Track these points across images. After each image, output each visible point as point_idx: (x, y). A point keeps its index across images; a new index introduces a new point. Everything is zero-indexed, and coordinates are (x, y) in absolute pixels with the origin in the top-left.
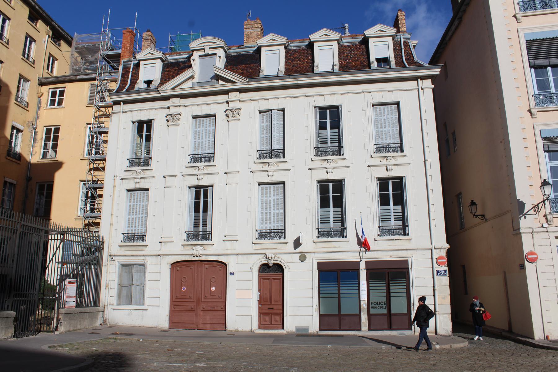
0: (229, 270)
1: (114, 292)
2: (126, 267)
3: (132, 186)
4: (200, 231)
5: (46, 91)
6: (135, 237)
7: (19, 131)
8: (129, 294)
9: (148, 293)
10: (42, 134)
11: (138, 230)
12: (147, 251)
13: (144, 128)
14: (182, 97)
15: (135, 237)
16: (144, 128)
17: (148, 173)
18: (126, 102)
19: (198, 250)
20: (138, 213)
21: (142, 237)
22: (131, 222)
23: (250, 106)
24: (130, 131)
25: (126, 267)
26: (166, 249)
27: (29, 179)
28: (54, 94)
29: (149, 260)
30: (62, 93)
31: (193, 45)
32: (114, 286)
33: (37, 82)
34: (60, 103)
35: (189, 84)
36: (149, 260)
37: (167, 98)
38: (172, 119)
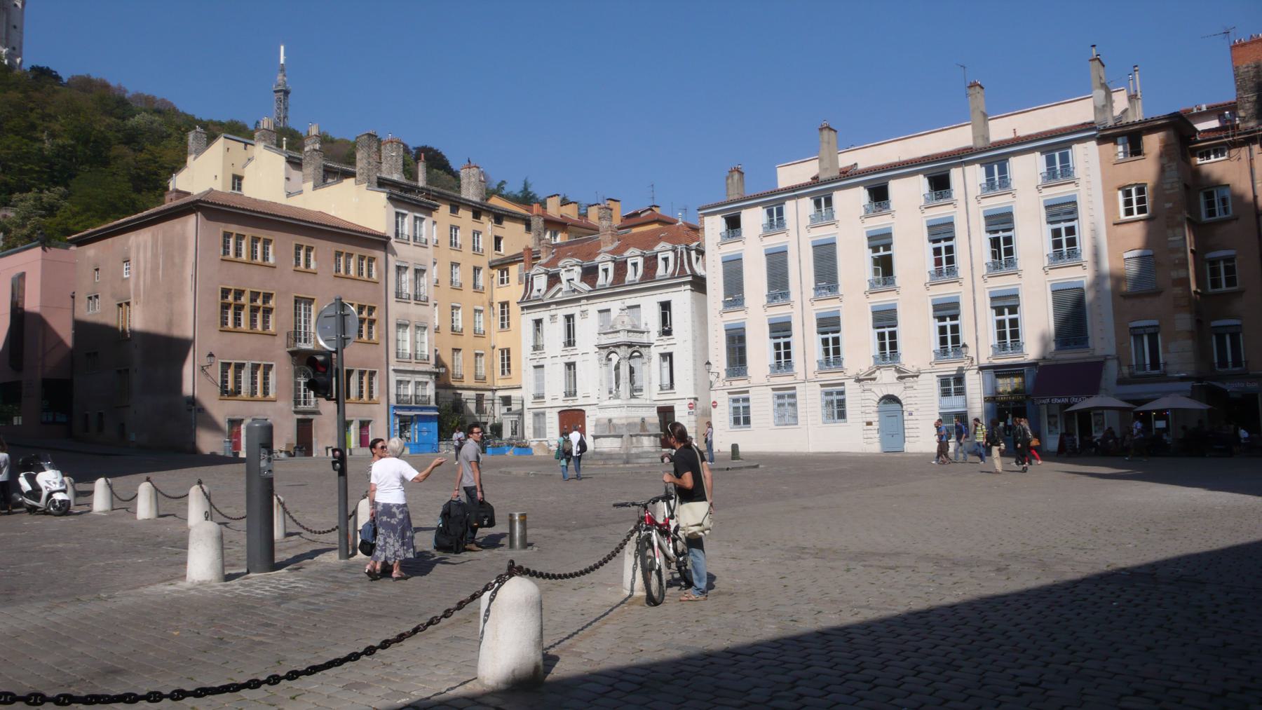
1: (531, 431)
4: (571, 393)
6: (539, 397)
7: (481, 311)
9: (548, 430)
10: (498, 309)
15: (539, 397)
16: (538, 322)
19: (570, 403)
20: (540, 382)
23: (593, 308)
25: (536, 415)
29: (547, 410)
31: (560, 264)
32: (531, 426)
35: (560, 295)
36: (547, 410)
37: (548, 305)
38: (553, 317)
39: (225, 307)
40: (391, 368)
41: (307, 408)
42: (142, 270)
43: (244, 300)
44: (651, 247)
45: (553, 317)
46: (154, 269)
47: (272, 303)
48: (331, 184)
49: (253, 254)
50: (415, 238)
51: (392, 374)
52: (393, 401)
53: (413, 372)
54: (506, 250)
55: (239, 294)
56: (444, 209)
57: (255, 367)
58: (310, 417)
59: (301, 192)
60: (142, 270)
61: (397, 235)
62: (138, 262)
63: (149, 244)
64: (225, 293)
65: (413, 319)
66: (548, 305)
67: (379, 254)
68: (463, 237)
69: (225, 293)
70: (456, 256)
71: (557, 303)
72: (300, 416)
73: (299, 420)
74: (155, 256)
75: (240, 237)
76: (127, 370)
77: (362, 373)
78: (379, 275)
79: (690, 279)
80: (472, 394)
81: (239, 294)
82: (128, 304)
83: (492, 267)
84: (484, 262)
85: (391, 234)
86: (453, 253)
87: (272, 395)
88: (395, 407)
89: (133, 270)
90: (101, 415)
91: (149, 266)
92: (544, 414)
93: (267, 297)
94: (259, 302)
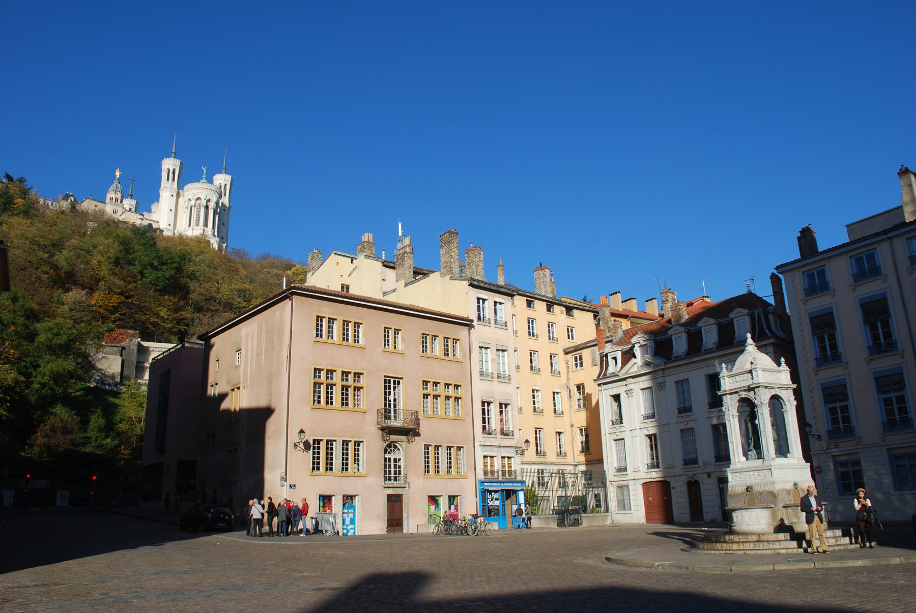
0: (672, 485)
2: (620, 487)
3: (616, 438)
5: (571, 358)
6: (622, 470)
8: (624, 505)
11: (623, 465)
12: (629, 477)
13: (617, 398)
14: (633, 377)
15: (622, 470)
17: (622, 429)
18: (604, 384)
21: (625, 469)
22: (619, 460)
24: (611, 401)
25: (620, 487)
26: (638, 476)
27: (572, 426)
28: (576, 358)
30: (581, 359)
33: (562, 353)
34: (581, 365)
36: (630, 483)
37: (625, 379)
38: (628, 392)
39: (317, 385)
40: (477, 444)
41: (396, 484)
42: (249, 356)
43: (337, 378)
44: (726, 316)
45: (628, 392)
46: (259, 355)
47: (363, 382)
48: (420, 279)
50: (496, 321)
51: (478, 449)
52: (481, 476)
54: (579, 340)
55: (330, 372)
56: (521, 301)
57: (345, 443)
58: (399, 491)
59: (394, 290)
60: (249, 356)
61: (479, 319)
62: (247, 350)
63: (256, 334)
64: (317, 371)
66: (625, 379)
67: (462, 332)
68: (540, 328)
69: (317, 371)
70: (532, 344)
72: (390, 492)
73: (389, 497)
74: (259, 343)
75: (331, 320)
76: (236, 449)
77: (449, 448)
78: (464, 356)
79: (772, 341)
81: (330, 372)
82: (238, 388)
83: (566, 353)
84: (559, 349)
85: (473, 316)
88: (483, 482)
89: (243, 359)
90: (215, 490)
91: (255, 352)
92: (627, 486)
93: (357, 375)
94: (351, 381)
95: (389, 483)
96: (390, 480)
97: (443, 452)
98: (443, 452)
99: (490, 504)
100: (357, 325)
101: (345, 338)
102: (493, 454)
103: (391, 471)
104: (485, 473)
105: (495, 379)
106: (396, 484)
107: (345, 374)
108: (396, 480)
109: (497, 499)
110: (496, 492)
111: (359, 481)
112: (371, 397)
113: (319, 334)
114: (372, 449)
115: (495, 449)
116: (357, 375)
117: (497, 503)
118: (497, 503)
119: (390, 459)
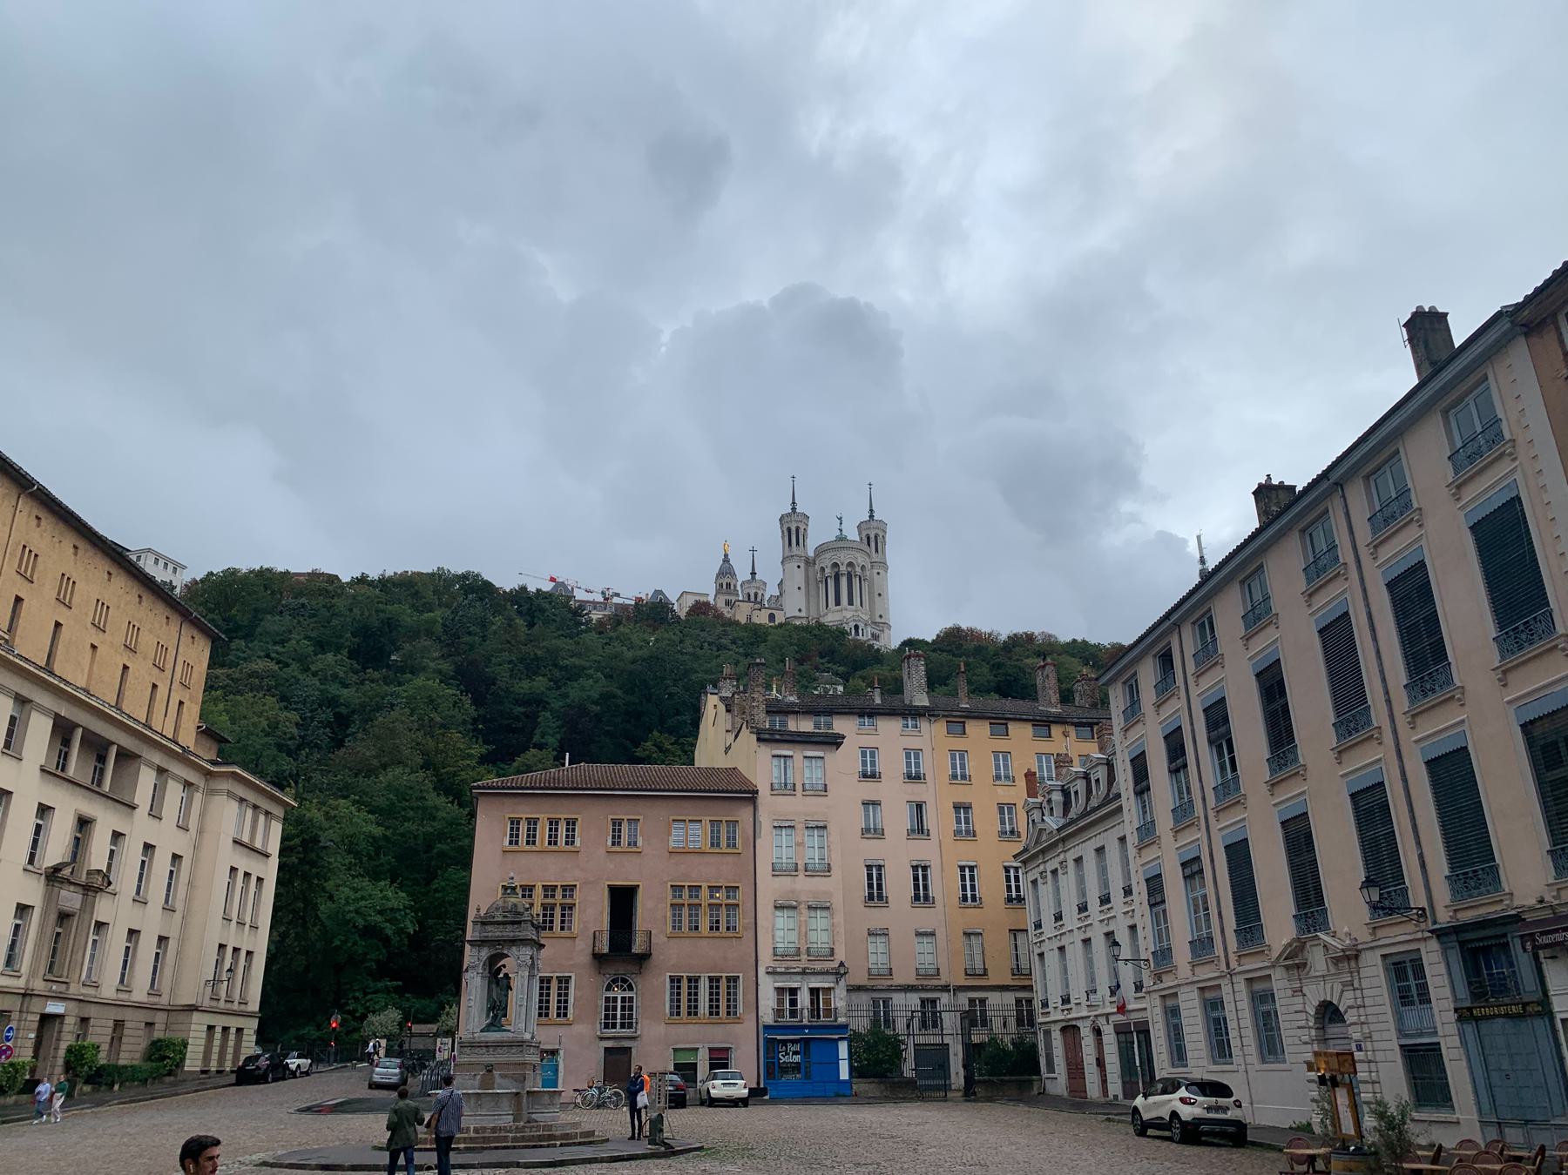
40: (762, 971)
49: (553, 841)
53: (804, 973)
58: (626, 1044)
65: (803, 898)
71: (1043, 851)
72: (610, 1044)
80: (963, 1000)
86: (1000, 790)
87: (570, 1016)
88: (767, 1027)
95: (610, 1032)
96: (614, 1026)
97: (704, 987)
98: (704, 987)
99: (783, 1060)
100: (571, 823)
101: (553, 841)
102: (795, 985)
103: (618, 1016)
104: (779, 1013)
105: (801, 873)
106: (626, 1032)
107: (549, 890)
108: (623, 1026)
109: (795, 1053)
110: (793, 1042)
111: (561, 1031)
112: (593, 915)
113: (514, 840)
114: (586, 991)
115: (799, 978)
116: (569, 889)
117: (797, 1058)
118: (797, 1058)
119: (615, 999)
